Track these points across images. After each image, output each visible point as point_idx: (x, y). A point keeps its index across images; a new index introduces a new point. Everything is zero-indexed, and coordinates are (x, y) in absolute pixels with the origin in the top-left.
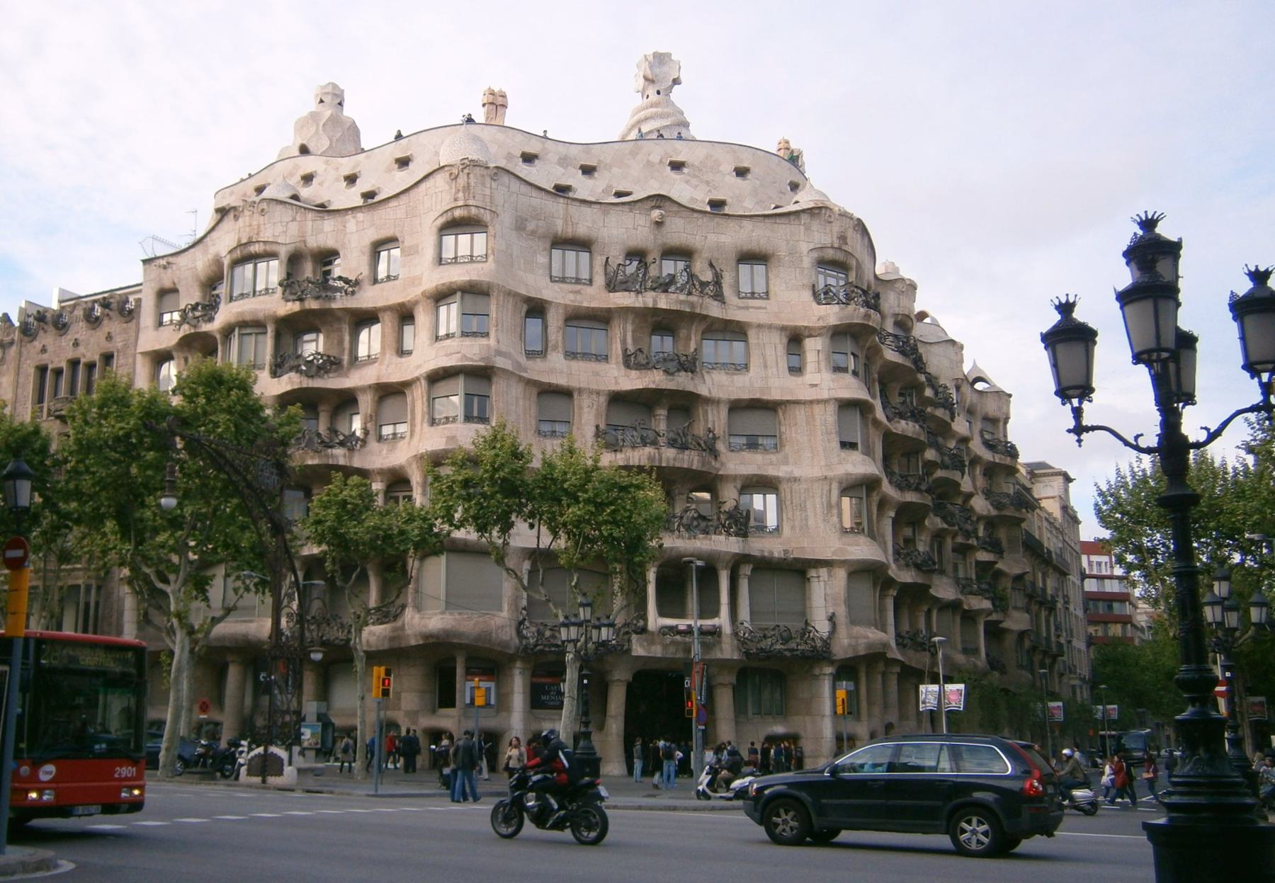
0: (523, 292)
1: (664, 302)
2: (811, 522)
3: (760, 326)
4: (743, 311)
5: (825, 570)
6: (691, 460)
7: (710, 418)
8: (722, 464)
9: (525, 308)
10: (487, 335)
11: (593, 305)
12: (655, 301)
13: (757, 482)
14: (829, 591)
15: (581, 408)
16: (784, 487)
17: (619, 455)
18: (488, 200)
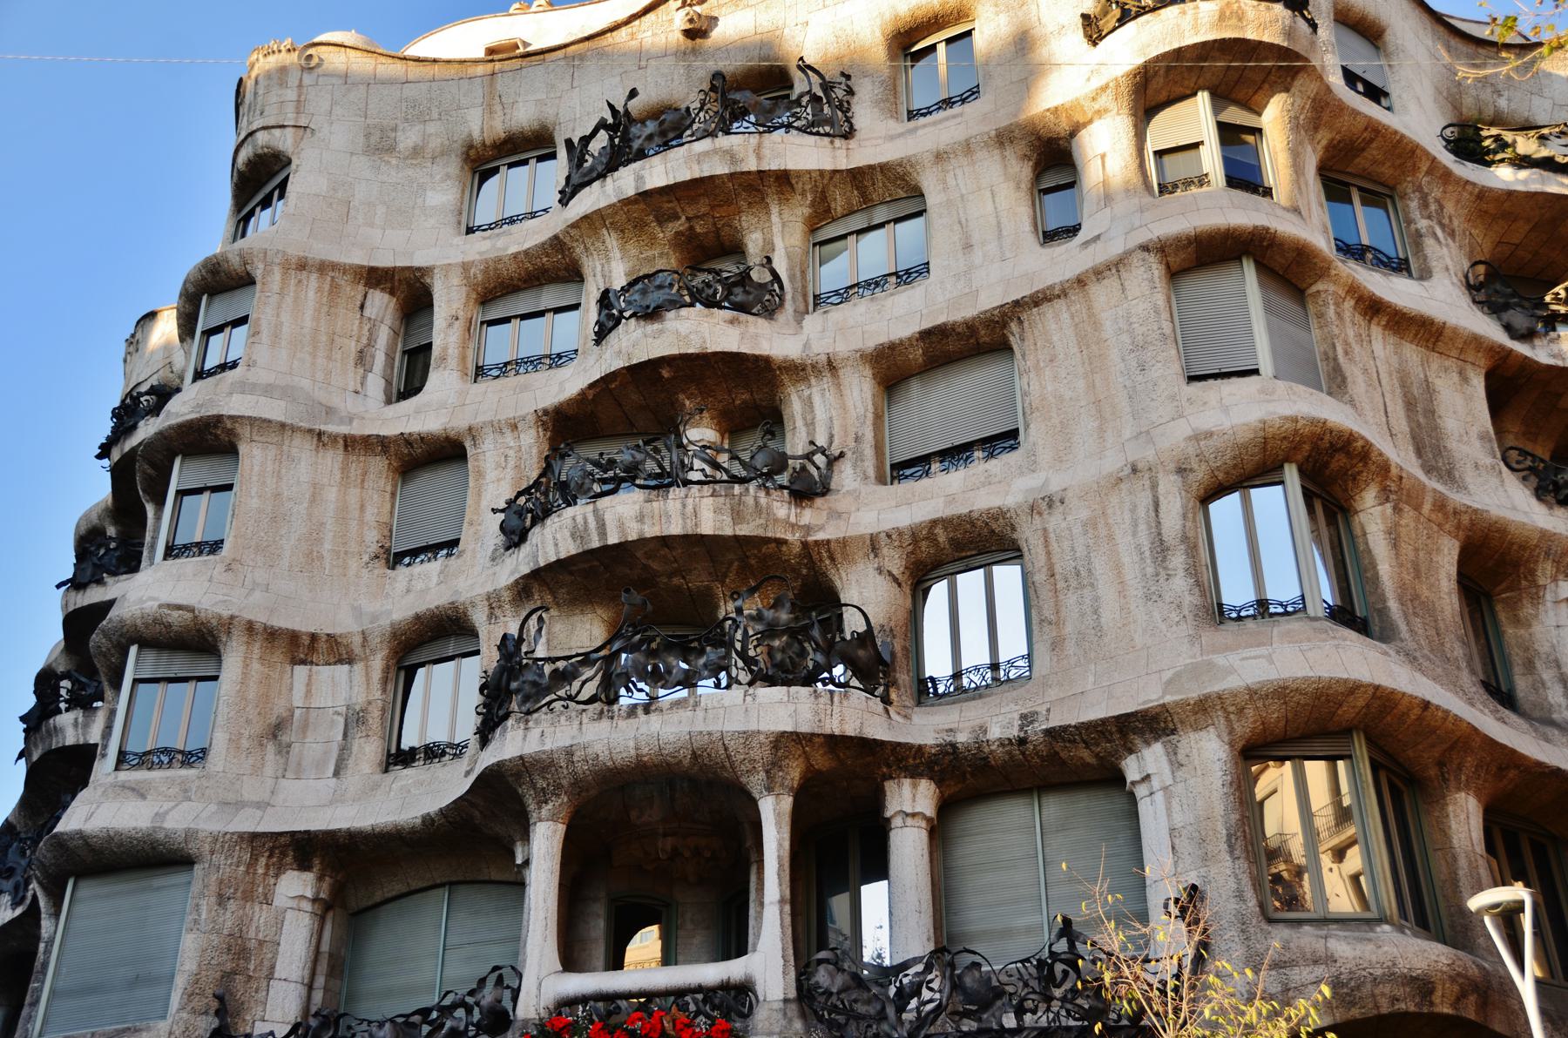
0: (359, 258)
1: (659, 171)
2: (1109, 615)
3: (940, 157)
4: (900, 142)
5: (1158, 748)
6: (697, 511)
7: (820, 414)
8: (835, 515)
9: (381, 304)
10: (234, 365)
11: (526, 246)
12: (639, 179)
13: (956, 544)
14: (1179, 820)
15: (480, 474)
16: (1027, 534)
17: (526, 549)
18: (290, 108)
